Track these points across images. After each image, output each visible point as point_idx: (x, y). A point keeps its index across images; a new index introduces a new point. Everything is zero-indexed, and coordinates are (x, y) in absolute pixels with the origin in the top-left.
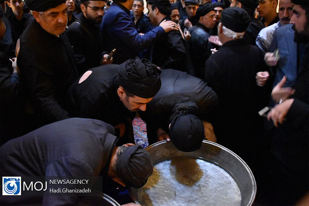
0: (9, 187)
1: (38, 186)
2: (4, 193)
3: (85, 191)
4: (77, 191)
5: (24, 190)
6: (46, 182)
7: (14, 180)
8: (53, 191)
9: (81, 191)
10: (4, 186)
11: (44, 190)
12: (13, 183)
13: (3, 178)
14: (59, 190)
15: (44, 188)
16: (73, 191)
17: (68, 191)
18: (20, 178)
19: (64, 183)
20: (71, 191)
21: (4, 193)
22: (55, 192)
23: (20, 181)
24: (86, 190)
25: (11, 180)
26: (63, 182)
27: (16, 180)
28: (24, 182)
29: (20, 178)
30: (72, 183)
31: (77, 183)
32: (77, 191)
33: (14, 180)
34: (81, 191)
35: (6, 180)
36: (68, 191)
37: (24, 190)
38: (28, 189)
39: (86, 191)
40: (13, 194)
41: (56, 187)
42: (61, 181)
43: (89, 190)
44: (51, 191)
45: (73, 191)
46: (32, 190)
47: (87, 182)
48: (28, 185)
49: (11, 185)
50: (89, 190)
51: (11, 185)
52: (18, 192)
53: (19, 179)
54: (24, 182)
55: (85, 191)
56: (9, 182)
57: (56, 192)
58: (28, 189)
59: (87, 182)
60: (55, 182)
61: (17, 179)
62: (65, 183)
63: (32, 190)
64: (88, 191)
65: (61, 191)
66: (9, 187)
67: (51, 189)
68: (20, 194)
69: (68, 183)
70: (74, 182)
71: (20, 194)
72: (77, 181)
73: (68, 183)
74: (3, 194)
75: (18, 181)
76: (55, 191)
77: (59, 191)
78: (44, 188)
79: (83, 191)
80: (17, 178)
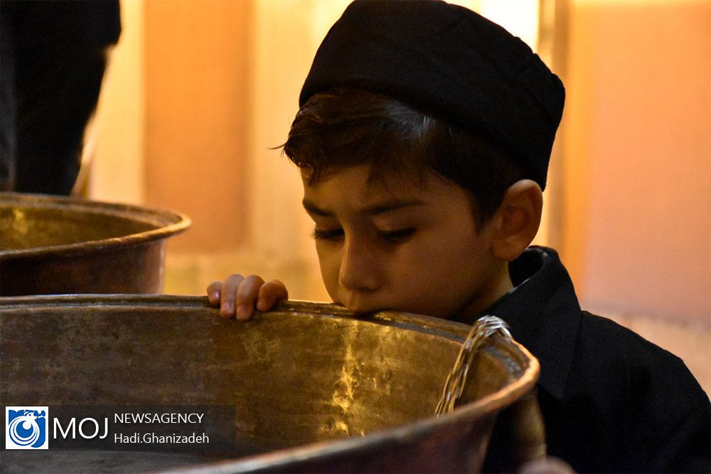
0: (20, 429)
1: (88, 428)
5: (55, 437)
6: (106, 419)
7: (32, 414)
8: (123, 439)
10: (10, 428)
11: (101, 437)
12: (29, 421)
13: (8, 409)
14: (135, 437)
15: (101, 432)
16: (169, 439)
17: (155, 439)
18: (46, 409)
19: (148, 421)
21: (10, 445)
22: (126, 441)
23: (47, 417)
24: (199, 438)
25: (26, 415)
27: (36, 413)
28: (56, 420)
29: (46, 409)
31: (177, 420)
33: (32, 414)
34: (186, 440)
35: (13, 415)
36: (155, 439)
37: (55, 437)
38: (65, 436)
40: (29, 447)
41: (128, 429)
42: (138, 420)
44: (118, 440)
45: (169, 439)
46: (74, 437)
47: (200, 418)
49: (26, 426)
51: (26, 426)
52: (41, 441)
53: (43, 413)
54: (56, 420)
56: (20, 419)
58: (65, 436)
59: (200, 418)
60: (126, 418)
61: (40, 413)
62: (148, 421)
63: (74, 437)
64: (202, 441)
65: (141, 439)
66: (20, 429)
67: (118, 436)
68: (45, 446)
69: (156, 422)
70: (171, 420)
72: (177, 416)
73: (156, 422)
74: (8, 447)
75: (42, 416)
76: (128, 440)
77: (136, 438)
78: (101, 432)
79: (191, 440)
80: (39, 409)
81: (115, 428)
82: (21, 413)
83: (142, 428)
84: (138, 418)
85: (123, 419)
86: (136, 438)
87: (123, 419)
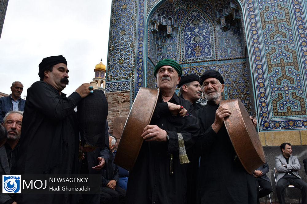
1: (38, 184)
2: (4, 192)
3: (84, 189)
4: (76, 189)
5: (24, 188)
6: (46, 180)
7: (14, 178)
8: (53, 189)
9: (80, 189)
10: (4, 184)
11: (44, 188)
12: (13, 181)
13: (3, 176)
14: (58, 188)
15: (44, 186)
16: (73, 189)
17: (67, 189)
18: (20, 176)
20: (70, 189)
21: (4, 192)
22: (54, 190)
23: (20, 180)
24: (86, 189)
25: (11, 179)
26: (62, 180)
27: (15, 178)
28: (24, 181)
29: (20, 176)
30: (72, 181)
31: (76, 181)
32: (76, 189)
33: (14, 178)
34: (80, 189)
35: (6, 179)
36: (67, 189)
37: (24, 188)
38: (28, 188)
39: (85, 189)
40: (13, 193)
41: (56, 185)
42: (60, 181)
43: (88, 189)
44: (51, 189)
45: (73, 189)
46: (32, 188)
47: (86, 180)
48: (28, 183)
49: (11, 183)
50: (88, 189)
51: (11, 183)
52: (18, 190)
53: (19, 178)
54: (24, 181)
55: (84, 189)
56: (8, 180)
57: (55, 190)
58: (28, 188)
59: (86, 180)
60: (54, 180)
61: (17, 178)
62: (64, 181)
63: (32, 188)
64: (87, 190)
65: (61, 189)
67: (51, 188)
68: (20, 192)
70: (74, 181)
71: (20, 192)
72: (76, 179)
74: (3, 192)
75: (18, 179)
76: (55, 189)
77: (59, 189)
78: (44, 186)
79: (83, 189)
80: (17, 176)
81: (49, 184)
82: (9, 178)
83: (62, 184)
84: (60, 180)
85: (53, 180)
86: (59, 189)
87: (53, 180)
